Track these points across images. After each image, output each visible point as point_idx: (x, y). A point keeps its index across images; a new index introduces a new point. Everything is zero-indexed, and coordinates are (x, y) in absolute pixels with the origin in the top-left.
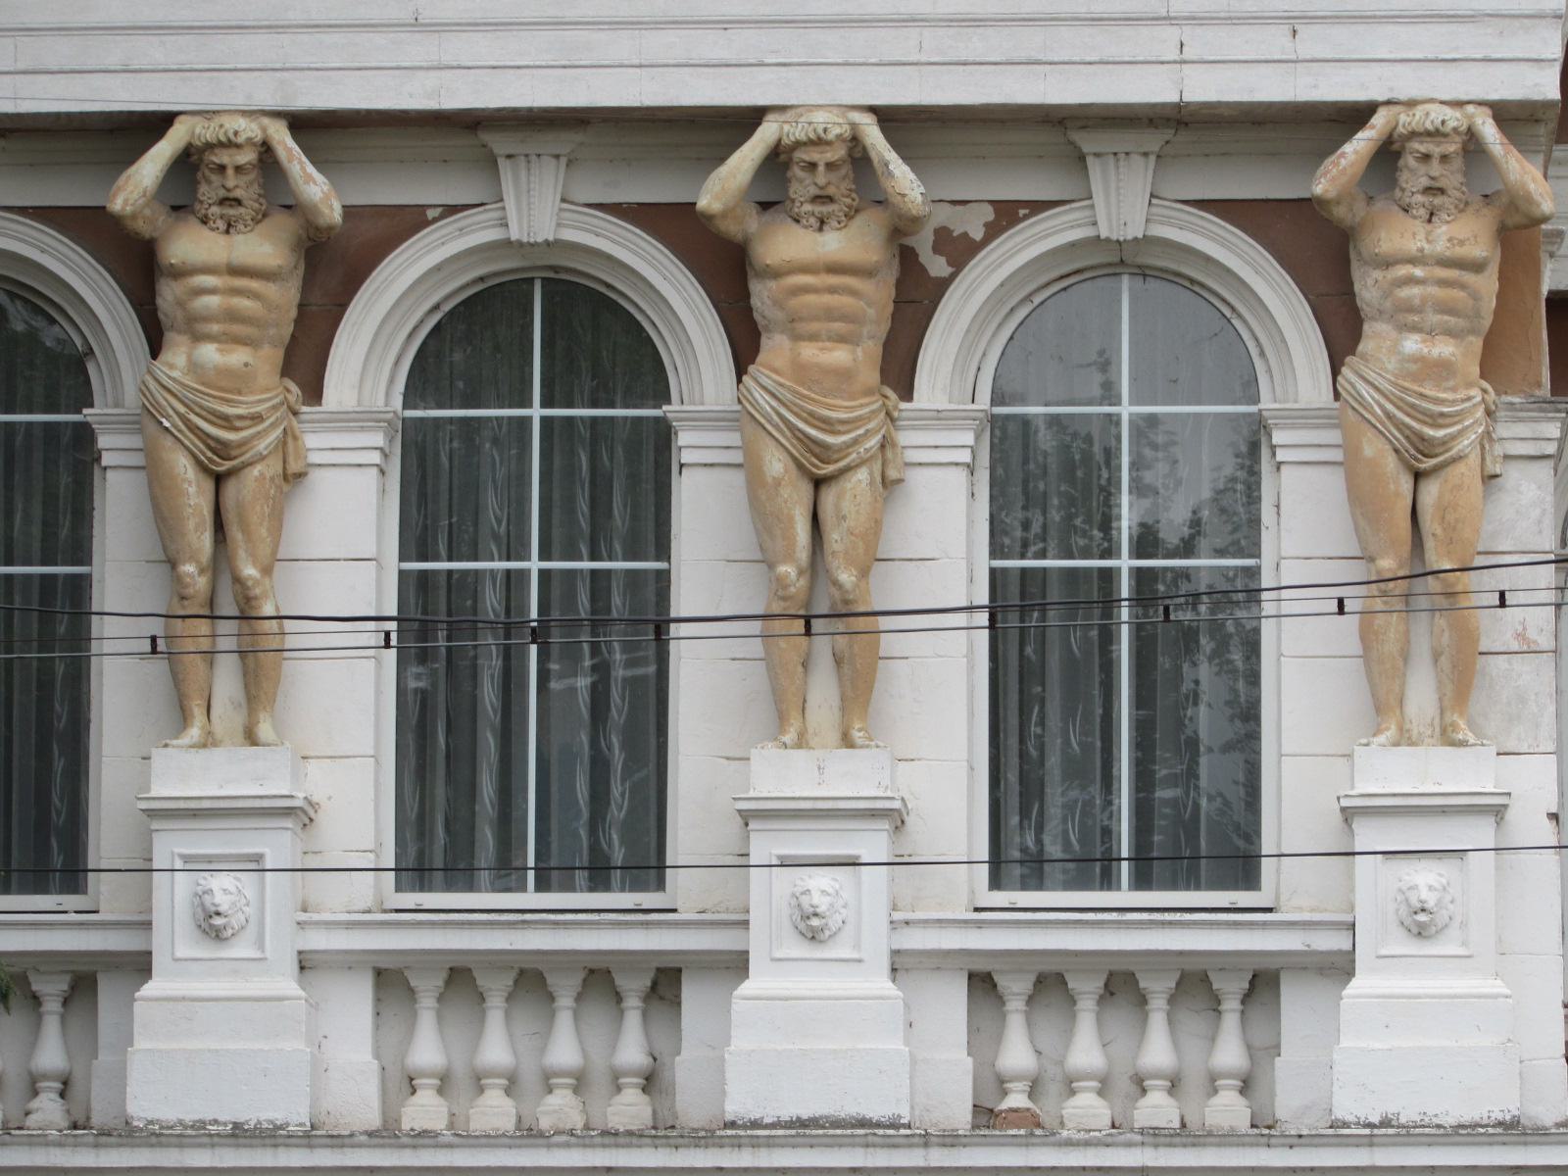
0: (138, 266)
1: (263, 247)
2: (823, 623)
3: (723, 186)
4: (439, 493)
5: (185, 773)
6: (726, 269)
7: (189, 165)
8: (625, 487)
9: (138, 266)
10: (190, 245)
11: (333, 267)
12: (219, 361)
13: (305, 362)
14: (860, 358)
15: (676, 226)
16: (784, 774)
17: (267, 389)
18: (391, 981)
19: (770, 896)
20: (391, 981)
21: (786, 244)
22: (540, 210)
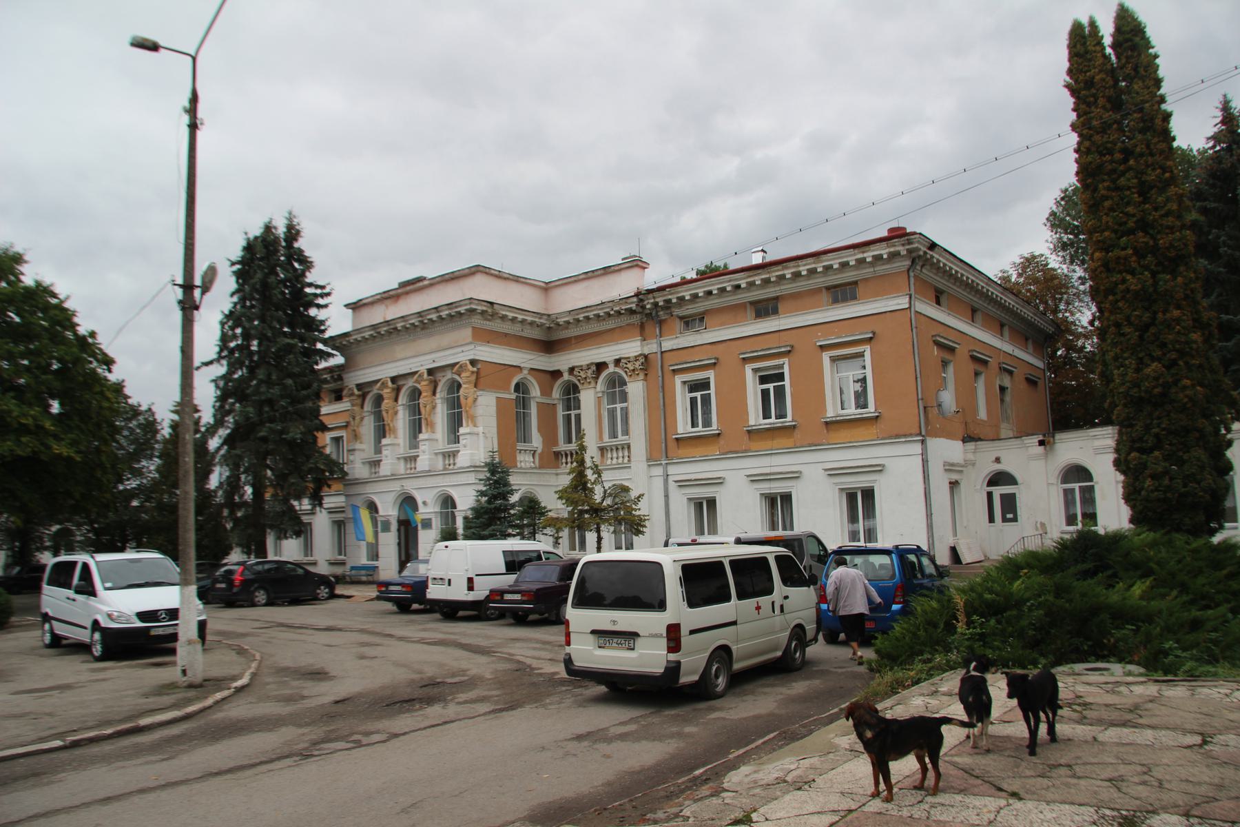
11: (398, 390)
14: (430, 393)
18: (405, 459)
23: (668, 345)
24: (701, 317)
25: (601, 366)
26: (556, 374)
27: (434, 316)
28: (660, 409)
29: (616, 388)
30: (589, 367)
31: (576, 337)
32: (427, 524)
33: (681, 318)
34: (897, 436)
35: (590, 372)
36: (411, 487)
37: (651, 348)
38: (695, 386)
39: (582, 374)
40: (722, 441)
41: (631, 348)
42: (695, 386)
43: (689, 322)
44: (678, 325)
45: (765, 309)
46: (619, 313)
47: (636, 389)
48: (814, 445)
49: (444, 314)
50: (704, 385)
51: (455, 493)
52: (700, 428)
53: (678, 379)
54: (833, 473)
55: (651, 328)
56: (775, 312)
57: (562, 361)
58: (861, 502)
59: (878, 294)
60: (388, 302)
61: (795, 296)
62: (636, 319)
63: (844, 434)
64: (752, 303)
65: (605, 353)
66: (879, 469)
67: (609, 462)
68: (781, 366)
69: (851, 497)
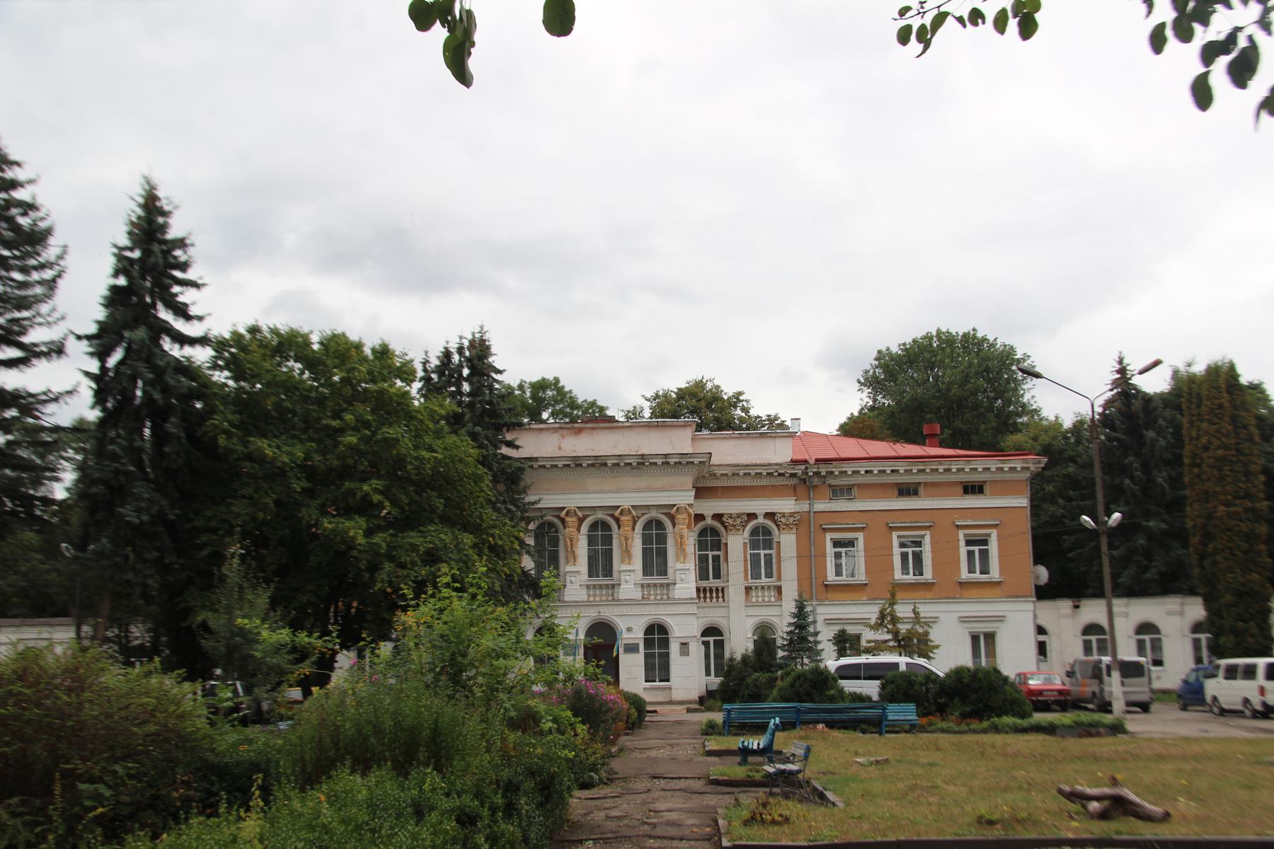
0: (563, 521)
1: (575, 519)
2: (627, 554)
3: (617, 513)
4: (591, 541)
5: (569, 568)
6: (617, 520)
7: (568, 512)
8: (608, 540)
9: (563, 521)
10: (568, 519)
11: (581, 521)
12: (571, 530)
13: (579, 530)
15: (612, 516)
16: (624, 567)
17: (575, 532)
18: (588, 587)
19: (623, 578)
20: (588, 587)
21: (623, 518)
22: (600, 515)
23: (820, 506)
24: (849, 488)
25: (752, 516)
26: (700, 517)
27: (659, 461)
28: (809, 559)
29: (762, 537)
30: (739, 516)
31: (723, 488)
32: (631, 648)
33: (830, 486)
34: (1015, 596)
35: (739, 521)
36: (609, 613)
37: (804, 506)
38: (837, 544)
39: (730, 521)
40: (868, 590)
41: (786, 505)
42: (837, 544)
43: (839, 492)
44: (828, 492)
45: (907, 490)
46: (780, 475)
47: (788, 542)
48: (950, 597)
49: (672, 461)
50: (851, 543)
51: (671, 622)
52: (844, 577)
53: (829, 536)
54: (964, 620)
55: (802, 490)
56: (916, 493)
57: (709, 507)
58: (984, 641)
59: (995, 494)
60: (565, 432)
61: (934, 484)
62: (795, 481)
63: (974, 592)
64: (896, 484)
65: (759, 506)
66: (1000, 619)
67: (754, 599)
68: (923, 536)
69: (975, 639)
